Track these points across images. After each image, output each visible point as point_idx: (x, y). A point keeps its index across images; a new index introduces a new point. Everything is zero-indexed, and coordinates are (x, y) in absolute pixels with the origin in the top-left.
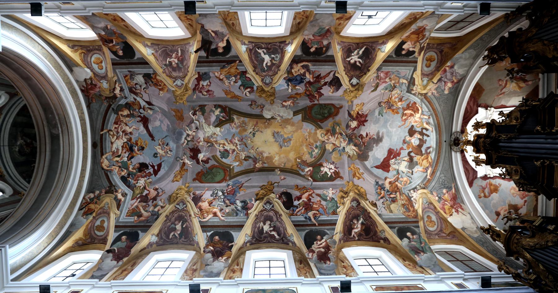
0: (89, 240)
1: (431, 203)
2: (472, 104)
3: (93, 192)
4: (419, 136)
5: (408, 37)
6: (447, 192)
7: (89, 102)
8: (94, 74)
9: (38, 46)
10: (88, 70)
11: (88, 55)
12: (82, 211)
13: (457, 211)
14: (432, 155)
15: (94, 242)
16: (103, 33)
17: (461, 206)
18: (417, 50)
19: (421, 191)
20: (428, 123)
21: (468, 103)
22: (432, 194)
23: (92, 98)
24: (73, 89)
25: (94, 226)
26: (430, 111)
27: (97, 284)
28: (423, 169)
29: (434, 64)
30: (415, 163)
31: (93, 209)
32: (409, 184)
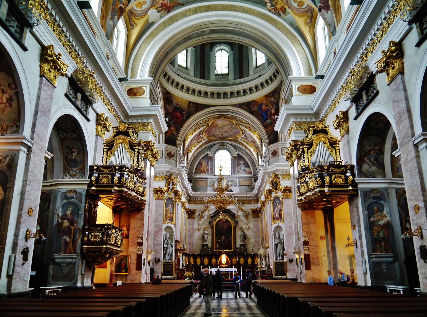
0: (309, 14)
3: (266, 3)
7: (178, 5)
8: (151, 7)
9: (140, 51)
10: (150, 12)
11: (135, 13)
12: (282, 14)
15: (312, 10)
16: (116, 17)
23: (174, 4)
24: (169, 20)
25: (297, 8)
27: (335, 38)
31: (282, 7)
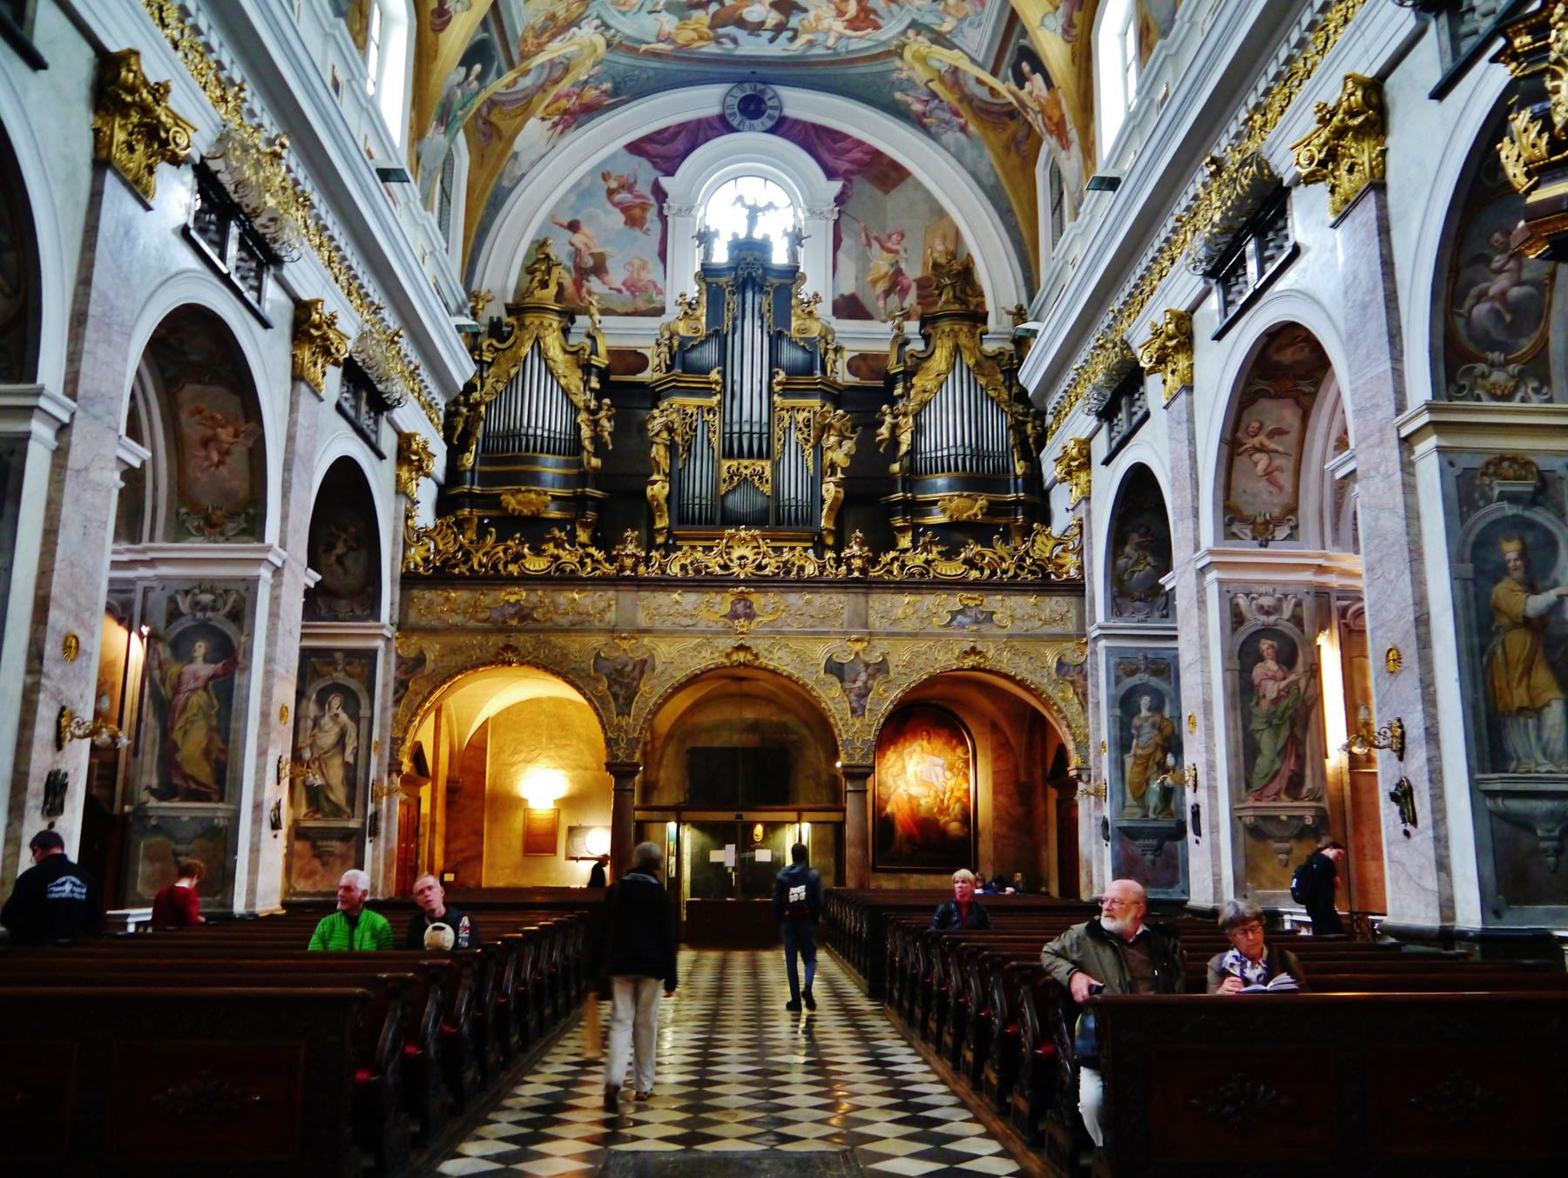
1: (567, 70)
2: (856, 154)
4: (771, 23)
5: (1058, 104)
6: (604, 92)
13: (555, 125)
14: (711, 48)
17: (569, 126)
18: (1023, 94)
19: (600, 41)
20: (811, 44)
21: (859, 143)
22: (594, 66)
26: (848, 52)
28: (669, 34)
29: (983, 93)
30: (687, 13)
32: (620, 12)
